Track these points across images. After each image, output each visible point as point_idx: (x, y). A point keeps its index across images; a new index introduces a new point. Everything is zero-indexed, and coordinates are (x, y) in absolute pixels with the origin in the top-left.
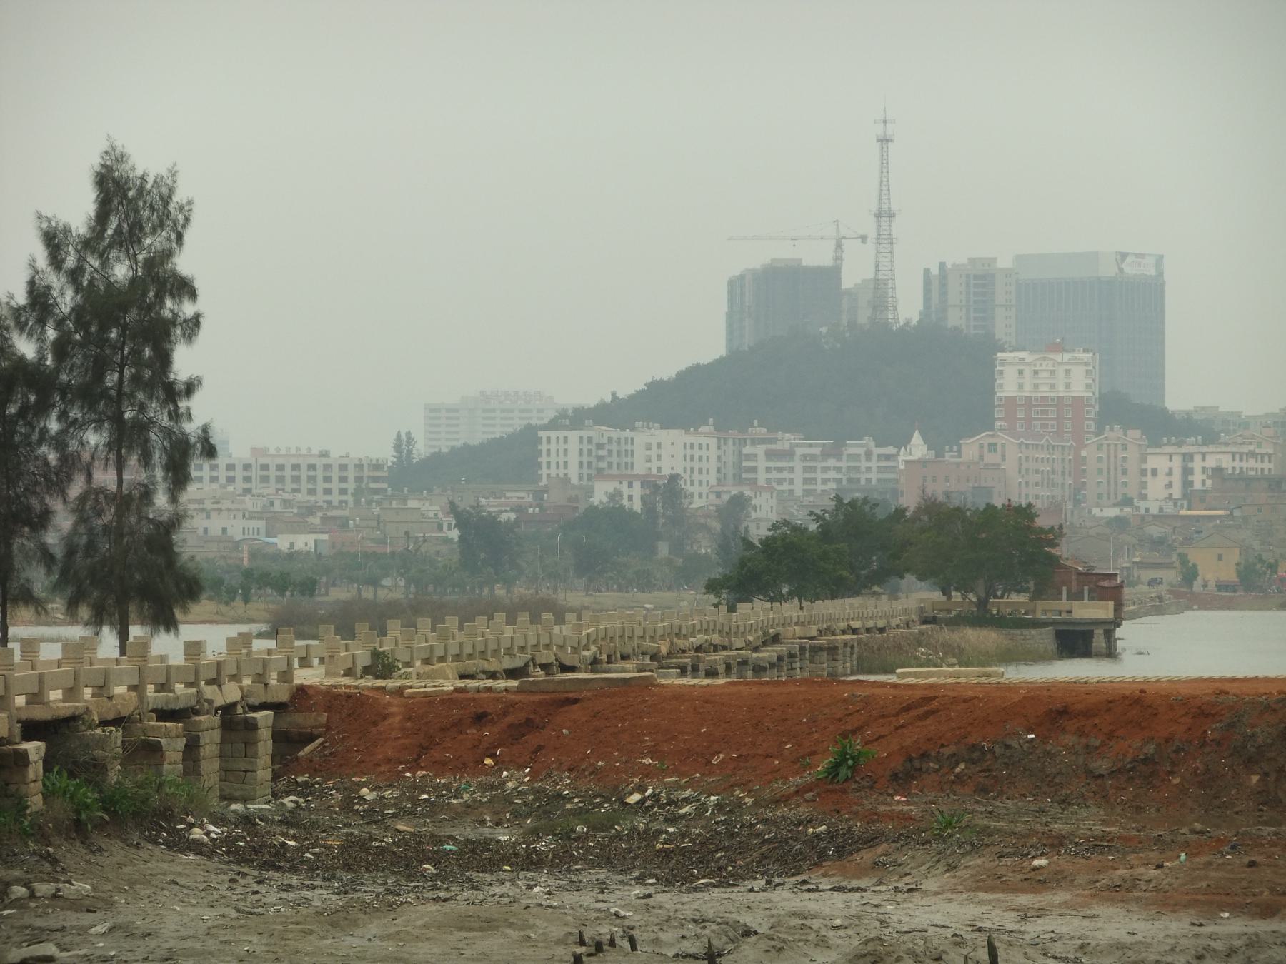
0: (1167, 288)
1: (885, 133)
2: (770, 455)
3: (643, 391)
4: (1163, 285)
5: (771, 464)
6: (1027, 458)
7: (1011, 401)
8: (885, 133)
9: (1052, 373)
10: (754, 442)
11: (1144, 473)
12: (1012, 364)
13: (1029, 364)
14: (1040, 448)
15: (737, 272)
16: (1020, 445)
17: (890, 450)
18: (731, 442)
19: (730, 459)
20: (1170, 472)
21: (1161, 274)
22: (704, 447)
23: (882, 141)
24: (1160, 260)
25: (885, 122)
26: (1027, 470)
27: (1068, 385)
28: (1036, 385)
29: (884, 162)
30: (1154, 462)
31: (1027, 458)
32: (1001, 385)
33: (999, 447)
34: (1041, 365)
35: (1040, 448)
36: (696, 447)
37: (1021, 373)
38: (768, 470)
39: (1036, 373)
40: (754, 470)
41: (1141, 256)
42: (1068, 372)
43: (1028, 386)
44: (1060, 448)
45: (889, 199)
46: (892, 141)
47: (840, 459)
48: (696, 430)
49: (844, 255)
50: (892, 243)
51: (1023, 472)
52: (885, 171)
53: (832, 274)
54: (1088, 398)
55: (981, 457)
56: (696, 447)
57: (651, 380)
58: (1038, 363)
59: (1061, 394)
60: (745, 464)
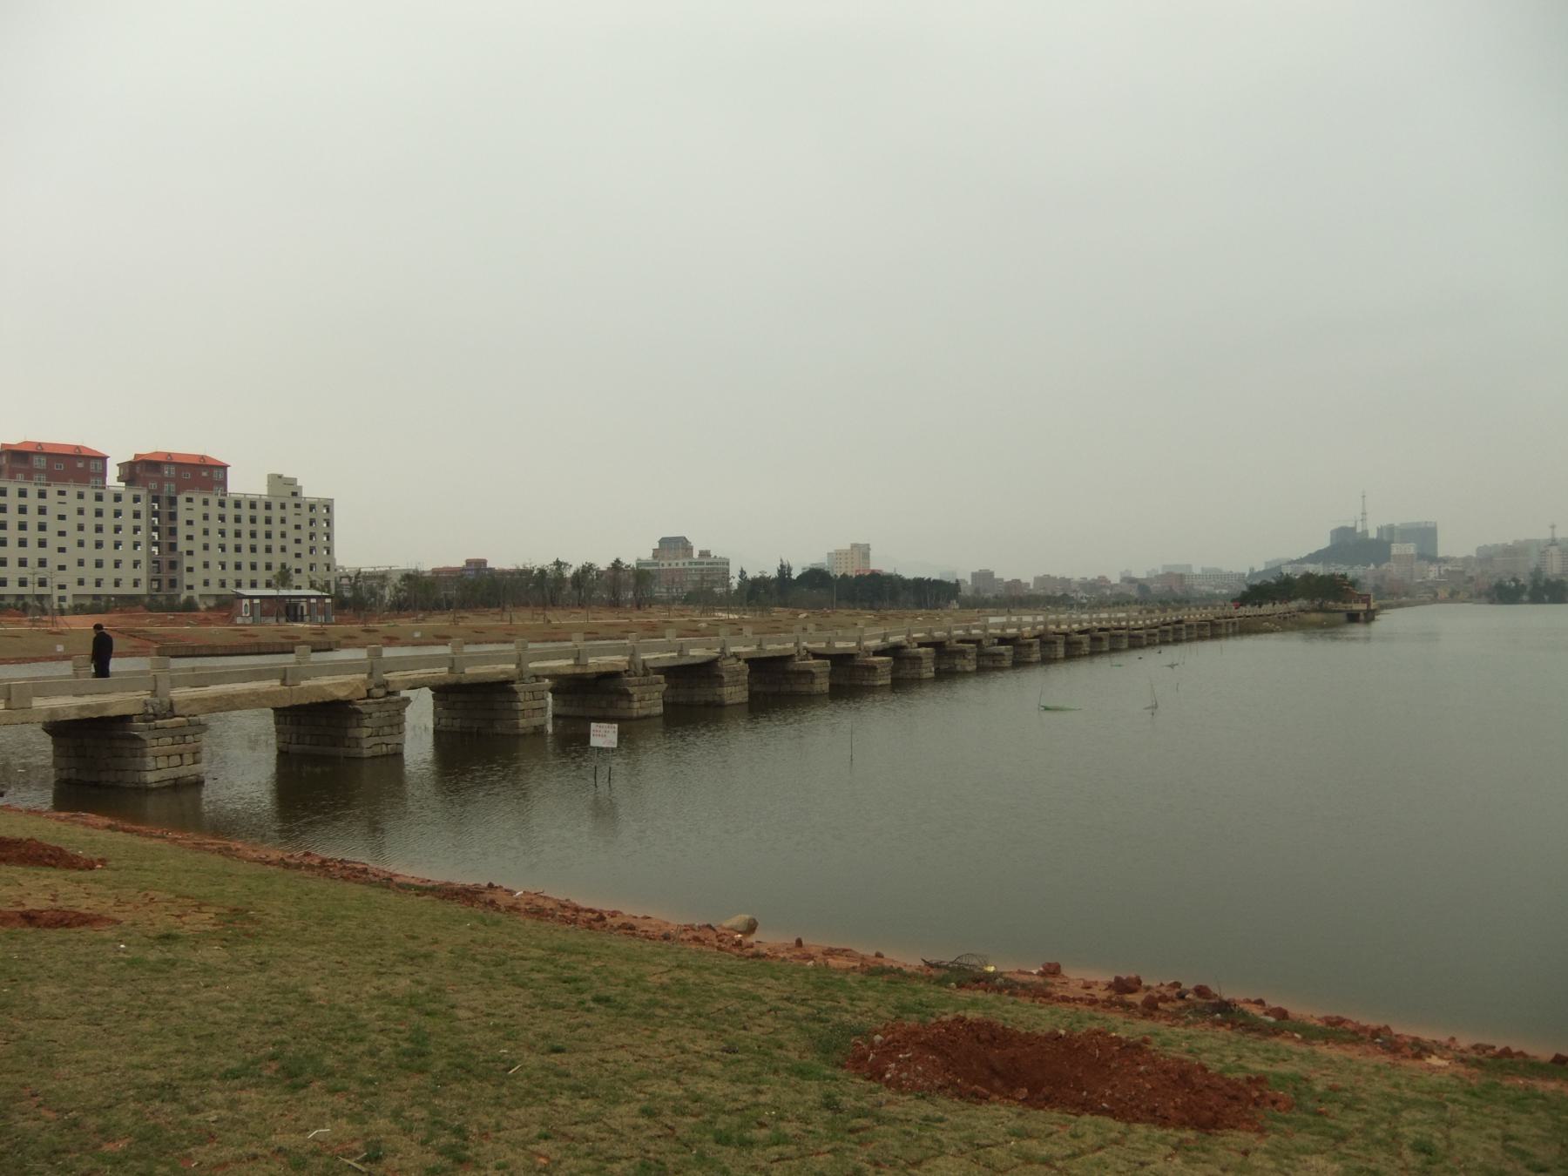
24: (1435, 523)
53: (1354, 529)
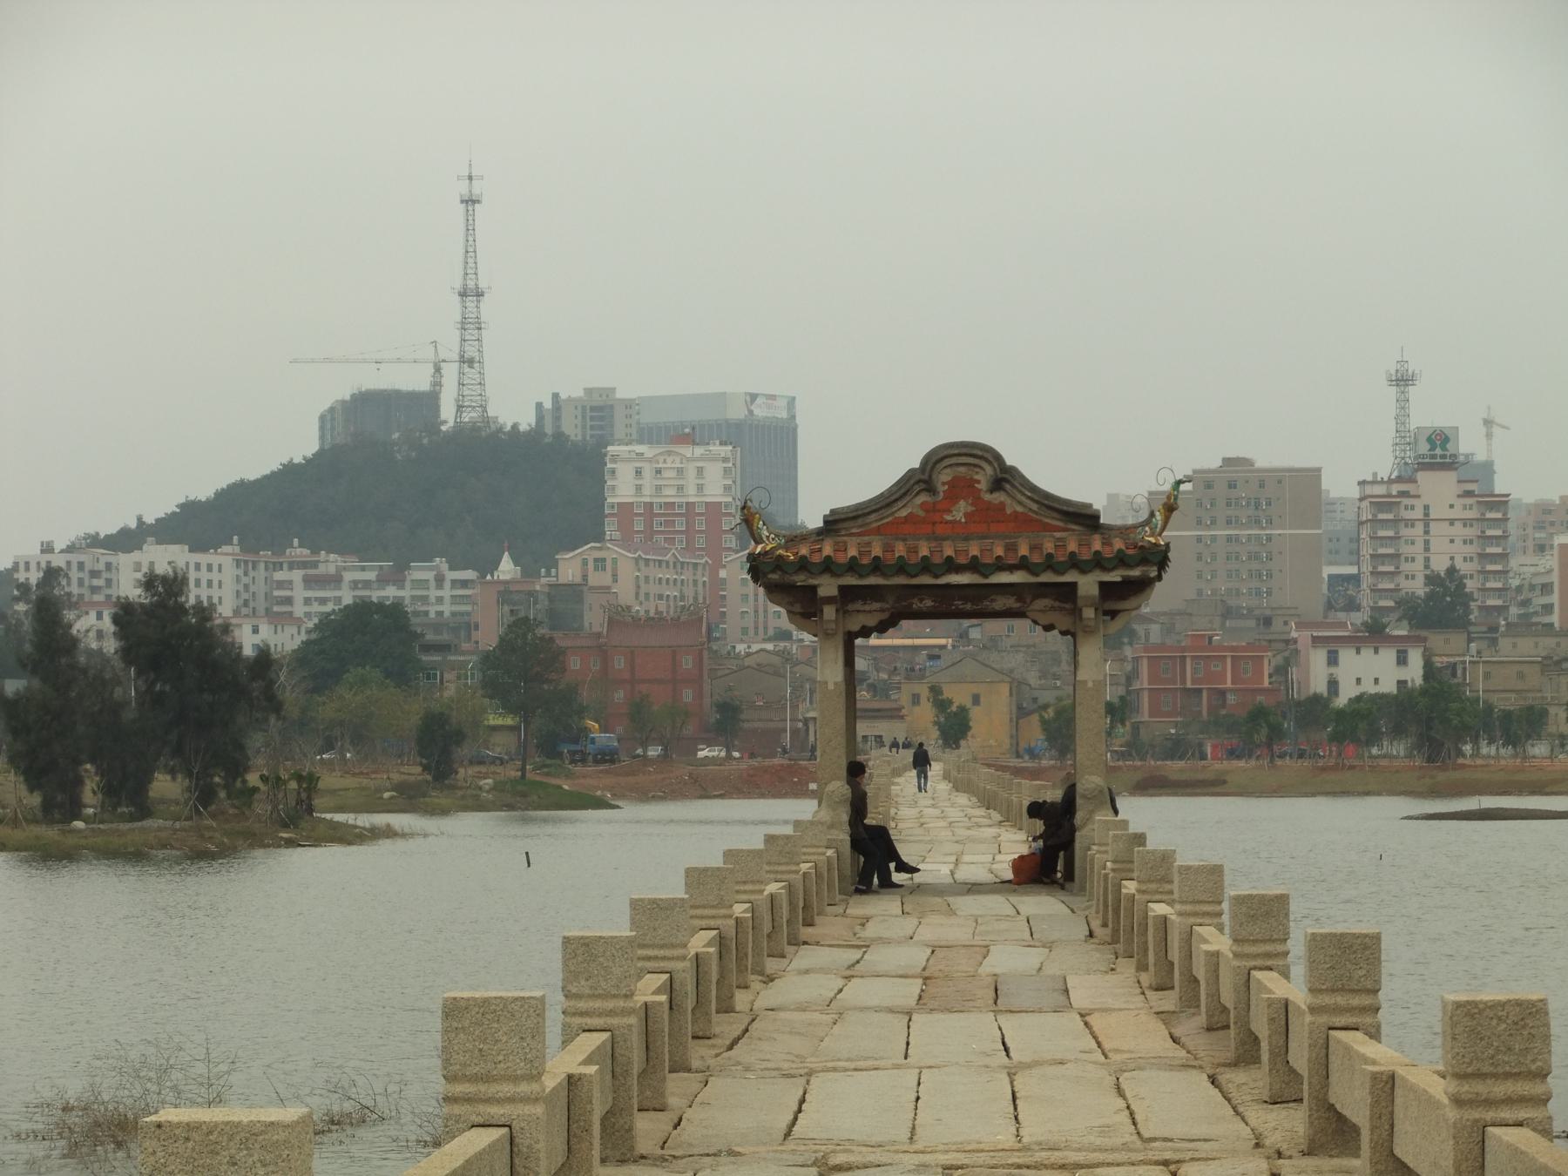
0: (799, 430)
1: (470, 191)
2: (309, 582)
3: (174, 513)
4: (795, 429)
5: (310, 594)
6: (647, 578)
7: (625, 508)
8: (470, 191)
9: (680, 471)
10: (292, 566)
12: (629, 460)
13: (650, 460)
14: (664, 565)
15: (327, 406)
16: (637, 560)
17: (470, 574)
18: (262, 566)
19: (260, 588)
21: (794, 417)
22: (215, 568)
23: (467, 202)
24: (792, 402)
25: (470, 178)
26: (647, 595)
27: (700, 488)
28: (659, 488)
29: (470, 229)
31: (647, 578)
32: (613, 487)
33: (609, 564)
34: (665, 461)
35: (664, 565)
36: (204, 568)
37: (638, 472)
38: (307, 601)
39: (659, 471)
40: (289, 601)
41: (773, 397)
42: (700, 471)
43: (647, 491)
44: (691, 567)
45: (476, 274)
46: (479, 202)
47: (400, 583)
48: (216, 551)
49: (444, 380)
50: (480, 329)
51: (642, 598)
52: (471, 239)
53: (428, 401)
54: (727, 505)
55: (585, 577)
56: (204, 568)
57: (182, 500)
58: (661, 459)
59: (691, 500)
60: (276, 593)
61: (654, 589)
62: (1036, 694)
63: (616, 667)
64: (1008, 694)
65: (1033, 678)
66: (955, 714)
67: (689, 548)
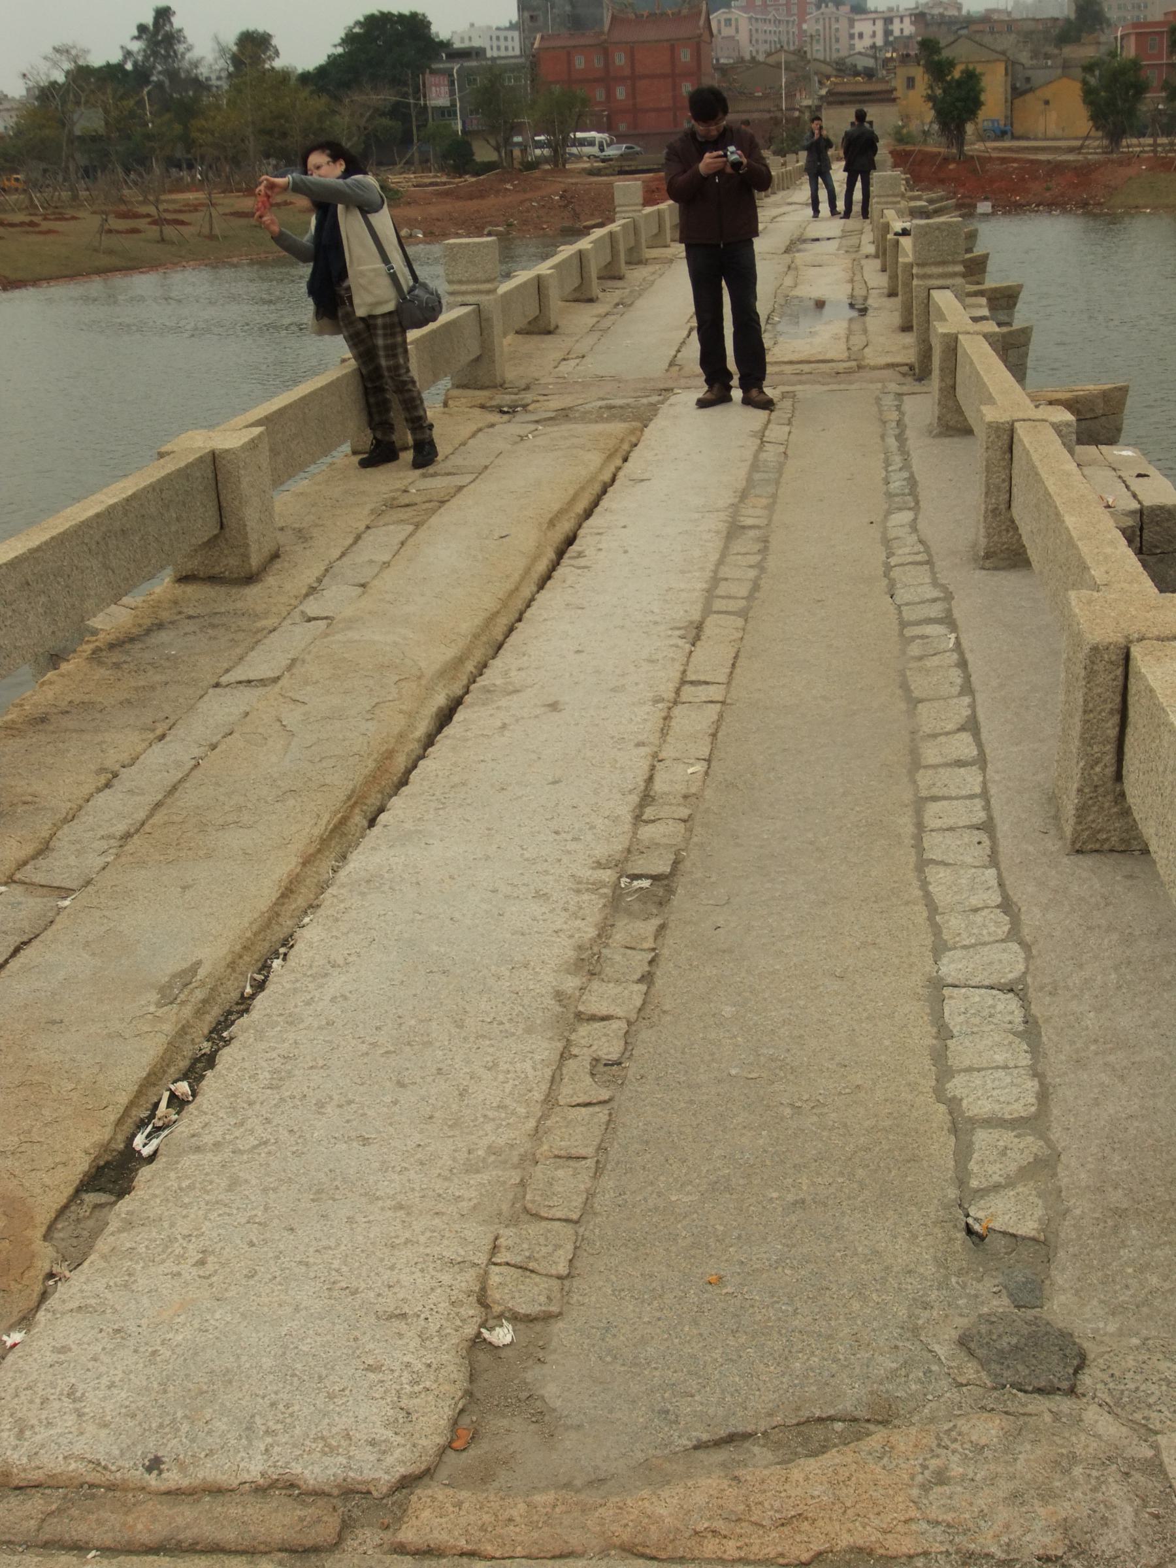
11: (852, 36)
20: (874, 35)
26: (757, 41)
30: (859, 27)
31: (757, 30)
33: (733, 22)
36: (502, 39)
56: (502, 39)
61: (761, 37)
62: (1029, 73)
63: (617, 62)
64: (1003, 72)
65: (1024, 57)
66: (959, 84)
67: (789, 13)
